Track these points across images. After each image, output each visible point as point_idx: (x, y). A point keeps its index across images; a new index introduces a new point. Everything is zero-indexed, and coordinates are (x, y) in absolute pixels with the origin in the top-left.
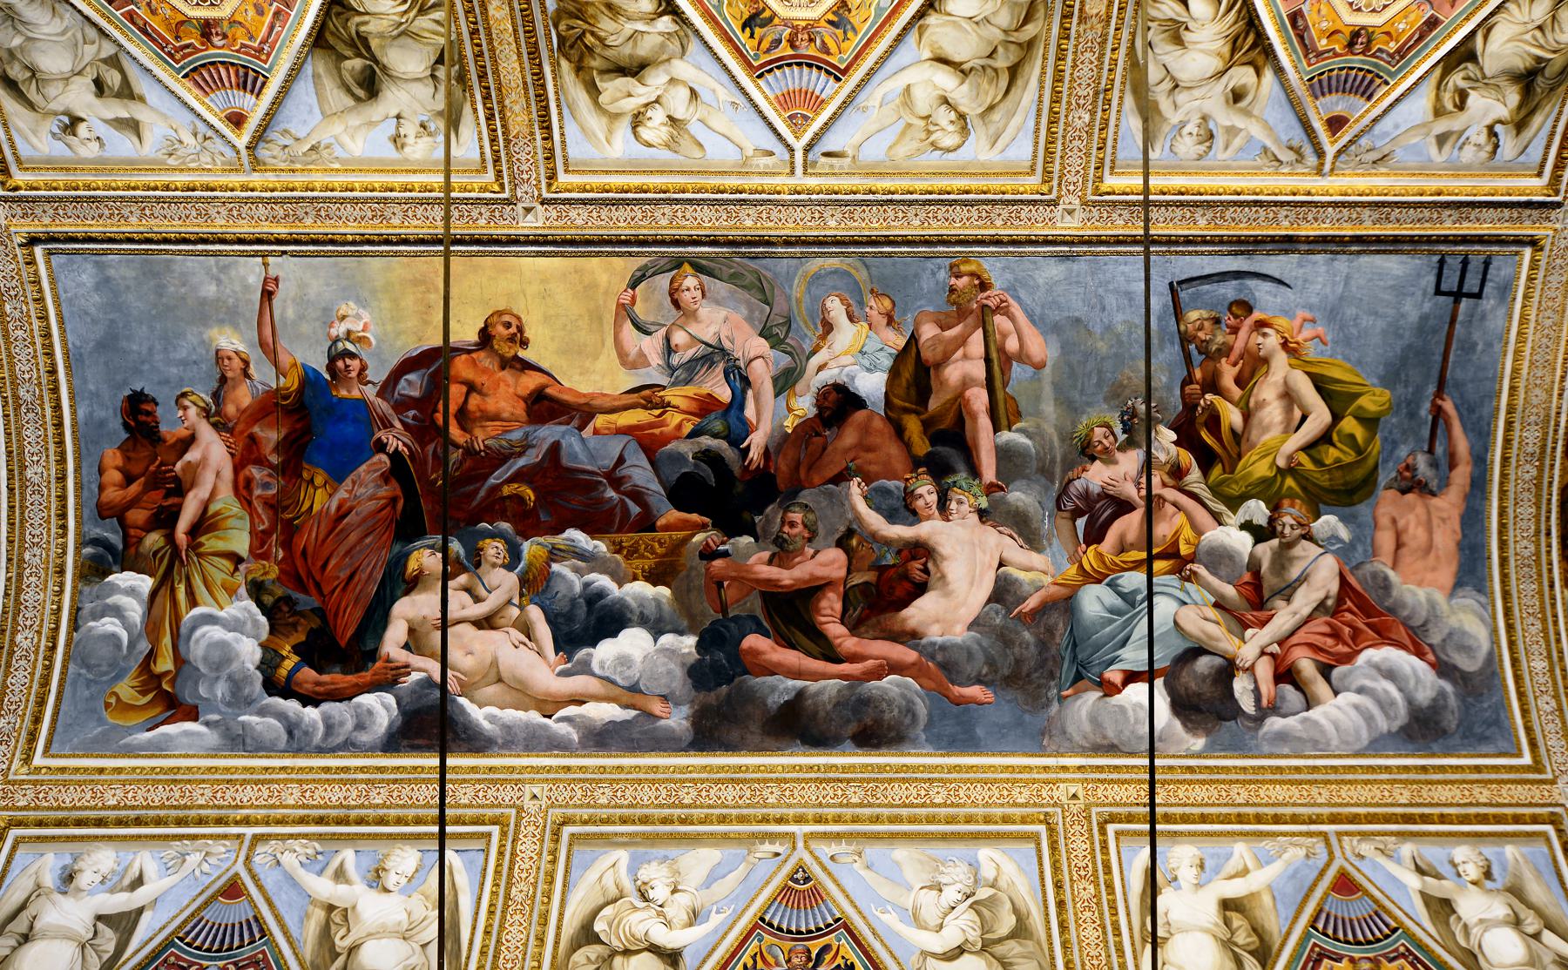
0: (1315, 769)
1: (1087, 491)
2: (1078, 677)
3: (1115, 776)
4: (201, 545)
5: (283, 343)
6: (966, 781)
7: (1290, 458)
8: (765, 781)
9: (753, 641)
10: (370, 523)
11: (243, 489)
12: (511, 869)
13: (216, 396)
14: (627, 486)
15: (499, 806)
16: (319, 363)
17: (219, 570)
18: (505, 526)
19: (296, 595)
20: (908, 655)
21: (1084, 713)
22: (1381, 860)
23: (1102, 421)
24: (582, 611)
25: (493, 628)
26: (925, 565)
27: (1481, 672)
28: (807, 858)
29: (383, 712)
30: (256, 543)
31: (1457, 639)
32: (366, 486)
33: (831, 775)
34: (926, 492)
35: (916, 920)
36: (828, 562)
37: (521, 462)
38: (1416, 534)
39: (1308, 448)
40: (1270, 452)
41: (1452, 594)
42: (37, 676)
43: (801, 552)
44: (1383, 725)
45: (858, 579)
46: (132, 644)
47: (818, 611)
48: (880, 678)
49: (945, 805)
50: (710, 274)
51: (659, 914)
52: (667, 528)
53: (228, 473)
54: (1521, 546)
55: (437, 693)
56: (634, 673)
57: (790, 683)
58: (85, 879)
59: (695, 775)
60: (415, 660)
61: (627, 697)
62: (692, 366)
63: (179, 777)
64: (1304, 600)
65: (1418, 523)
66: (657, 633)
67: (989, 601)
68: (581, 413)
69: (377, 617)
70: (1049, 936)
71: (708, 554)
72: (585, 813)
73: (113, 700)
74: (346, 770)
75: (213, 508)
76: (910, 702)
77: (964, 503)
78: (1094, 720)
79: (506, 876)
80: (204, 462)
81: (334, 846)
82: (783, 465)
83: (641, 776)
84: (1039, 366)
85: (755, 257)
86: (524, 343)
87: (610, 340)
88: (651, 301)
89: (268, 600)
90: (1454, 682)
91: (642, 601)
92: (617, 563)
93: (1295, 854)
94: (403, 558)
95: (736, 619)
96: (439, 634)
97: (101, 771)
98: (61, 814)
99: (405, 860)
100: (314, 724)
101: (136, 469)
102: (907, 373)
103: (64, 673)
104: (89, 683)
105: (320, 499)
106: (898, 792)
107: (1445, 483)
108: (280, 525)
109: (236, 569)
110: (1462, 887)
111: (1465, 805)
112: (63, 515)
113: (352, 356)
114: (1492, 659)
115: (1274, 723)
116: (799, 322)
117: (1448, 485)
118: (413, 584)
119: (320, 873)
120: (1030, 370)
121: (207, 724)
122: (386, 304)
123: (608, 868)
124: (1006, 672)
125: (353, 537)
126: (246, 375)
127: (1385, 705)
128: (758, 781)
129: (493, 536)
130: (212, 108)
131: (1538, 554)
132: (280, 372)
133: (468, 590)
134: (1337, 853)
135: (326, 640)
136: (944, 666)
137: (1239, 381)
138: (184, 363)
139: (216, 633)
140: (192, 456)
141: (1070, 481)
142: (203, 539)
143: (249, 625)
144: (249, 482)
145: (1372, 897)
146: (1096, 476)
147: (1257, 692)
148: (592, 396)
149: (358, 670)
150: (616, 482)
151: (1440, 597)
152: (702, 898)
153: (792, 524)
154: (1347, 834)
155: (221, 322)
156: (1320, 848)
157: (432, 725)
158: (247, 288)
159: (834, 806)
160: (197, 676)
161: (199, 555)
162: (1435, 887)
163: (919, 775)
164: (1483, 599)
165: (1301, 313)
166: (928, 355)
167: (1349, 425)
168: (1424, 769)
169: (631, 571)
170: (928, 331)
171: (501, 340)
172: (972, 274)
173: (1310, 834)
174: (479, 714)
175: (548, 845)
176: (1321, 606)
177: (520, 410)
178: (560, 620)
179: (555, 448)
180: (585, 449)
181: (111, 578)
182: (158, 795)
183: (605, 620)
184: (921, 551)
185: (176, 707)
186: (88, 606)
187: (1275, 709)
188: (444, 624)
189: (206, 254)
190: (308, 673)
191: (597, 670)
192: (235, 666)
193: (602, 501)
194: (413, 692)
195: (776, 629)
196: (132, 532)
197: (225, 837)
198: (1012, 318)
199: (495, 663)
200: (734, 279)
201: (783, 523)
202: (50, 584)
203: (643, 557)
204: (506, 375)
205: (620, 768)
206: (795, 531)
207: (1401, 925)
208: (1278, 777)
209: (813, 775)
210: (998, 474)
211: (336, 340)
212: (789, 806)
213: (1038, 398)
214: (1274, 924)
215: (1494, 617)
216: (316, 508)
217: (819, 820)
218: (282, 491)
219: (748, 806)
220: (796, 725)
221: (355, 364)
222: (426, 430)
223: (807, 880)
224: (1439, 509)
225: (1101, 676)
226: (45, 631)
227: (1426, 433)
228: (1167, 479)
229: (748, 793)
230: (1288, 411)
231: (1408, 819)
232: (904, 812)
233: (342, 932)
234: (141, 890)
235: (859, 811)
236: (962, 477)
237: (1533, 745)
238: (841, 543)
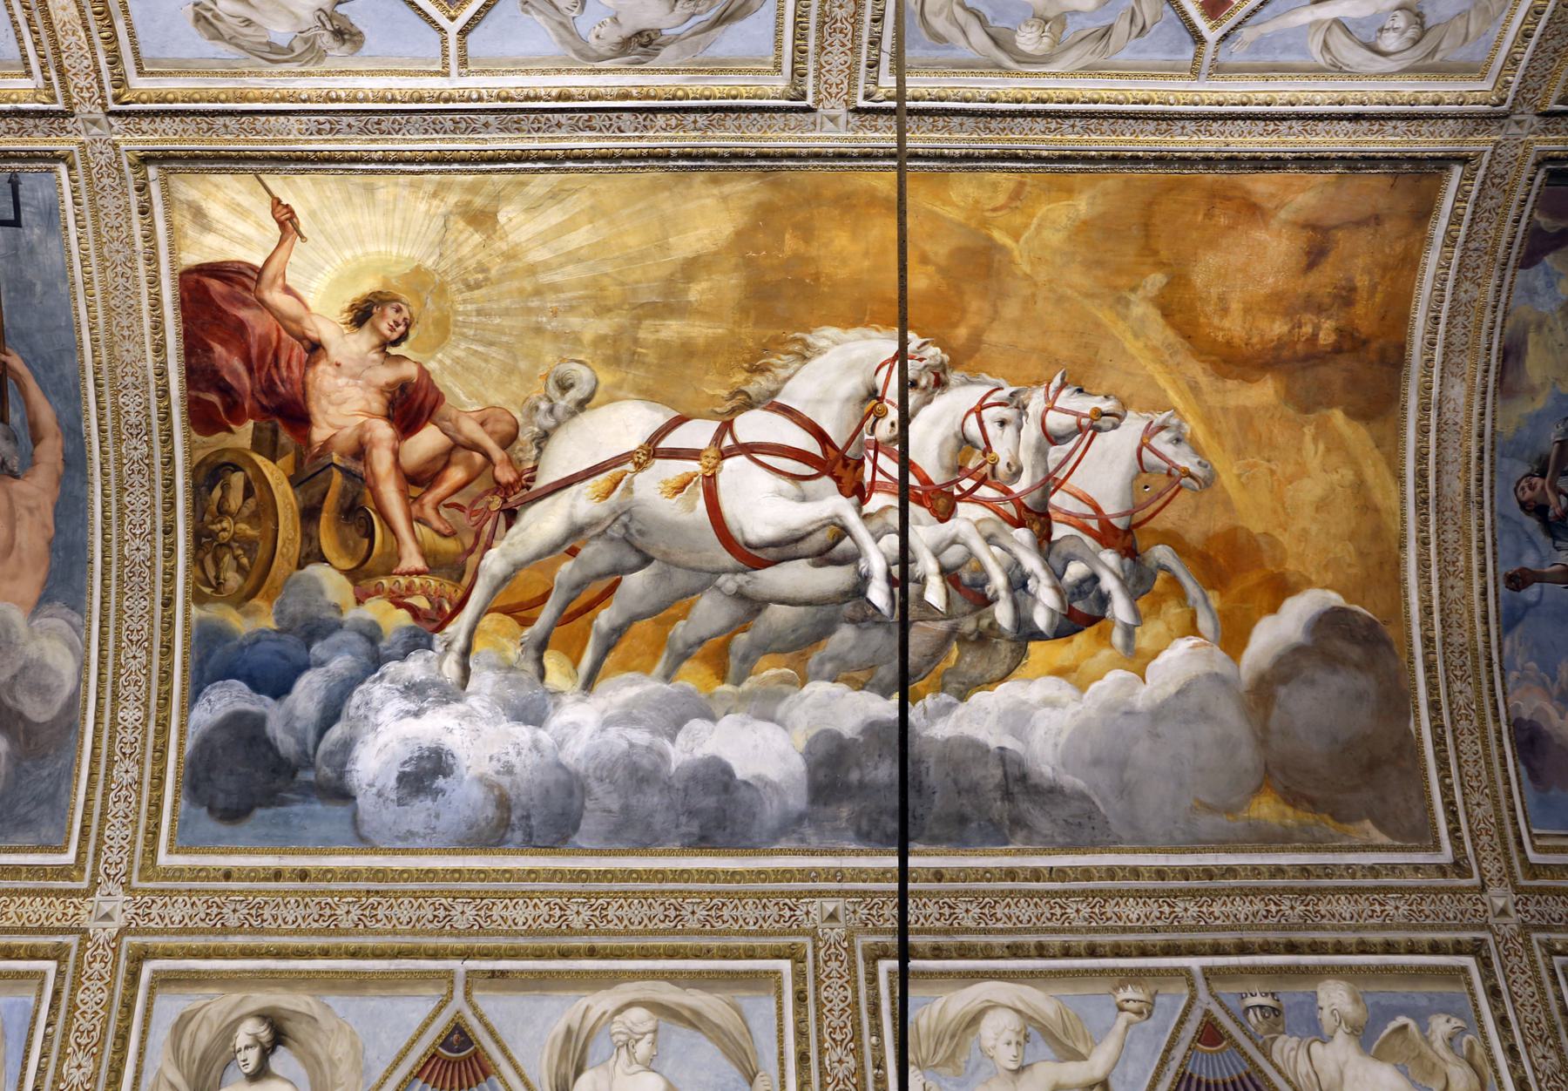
27: (54, 723)
41: (34, 613)
107: (31, 462)
114: (74, 705)
117: (33, 464)
164: (76, 619)
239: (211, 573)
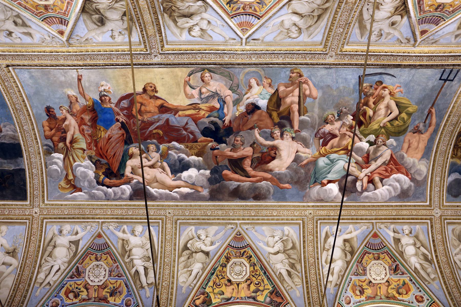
0: (374, 206)
1: (324, 132)
2: (315, 182)
3: (322, 208)
4: (73, 146)
5: (86, 93)
6: (282, 210)
7: (385, 124)
8: (229, 209)
9: (226, 172)
10: (118, 140)
11: (82, 132)
12: (165, 232)
13: (70, 107)
14: (189, 130)
15: (161, 215)
16: (97, 98)
17: (80, 153)
18: (155, 141)
19: (101, 159)
20: (268, 176)
21: (315, 191)
22: (385, 229)
23: (331, 112)
24: (178, 164)
25: (154, 168)
26: (275, 152)
27: (422, 180)
28: (240, 230)
29: (128, 190)
30: (88, 146)
31: (418, 172)
32: (115, 131)
33: (247, 208)
34: (277, 132)
35: (268, 245)
36: (247, 151)
37: (158, 124)
38: (415, 144)
39: (390, 121)
40: (379, 122)
41: (420, 160)
42: (40, 181)
43: (240, 148)
44: (393, 194)
45: (256, 156)
46: (62, 172)
47: (244, 164)
48: (261, 182)
49: (276, 216)
50: (214, 72)
51: (203, 243)
52: (201, 142)
53: (77, 127)
54: (442, 147)
55: (142, 185)
56: (193, 180)
57: (236, 183)
58: (64, 232)
59: (211, 208)
60: (135, 176)
61: (192, 186)
62: (208, 99)
63: (81, 207)
64: (380, 162)
65: (416, 141)
66: (199, 169)
67: (293, 162)
68: (175, 111)
69: (123, 165)
70: (300, 249)
71: (213, 149)
72: (183, 217)
73: (60, 186)
74: (121, 205)
75: (75, 137)
76: (269, 188)
77: (288, 135)
78: (318, 193)
79: (164, 233)
80: (70, 124)
81: (121, 225)
82: (234, 125)
83: (197, 208)
84: (315, 98)
85: (229, 68)
86: (156, 92)
87: (182, 91)
88: (195, 79)
89: (94, 161)
90: (414, 183)
91: (194, 161)
92: (187, 151)
93: (364, 227)
94: (127, 150)
95: (221, 166)
96: (141, 170)
97: (62, 205)
98: (55, 216)
99: (139, 228)
100: (111, 193)
101: (52, 126)
102: (274, 100)
103: (47, 179)
104: (53, 182)
105: (104, 134)
106: (264, 213)
108: (94, 141)
109: (84, 152)
110: (403, 236)
111: (409, 215)
112: (36, 139)
113: (106, 96)
115: (366, 194)
116: (241, 86)
118: (131, 156)
119: (119, 231)
120: (312, 100)
121: (85, 193)
122: (114, 82)
123: (190, 231)
124: (296, 180)
125: (113, 144)
126: (77, 101)
127: (395, 189)
128: (227, 209)
129: (152, 144)
130: (53, 30)
131: (446, 150)
132: (87, 100)
133: (146, 158)
134: (375, 228)
135: (111, 172)
136: (278, 179)
137: (374, 103)
138: (59, 98)
139: (82, 169)
140: (67, 123)
141: (320, 129)
142: (74, 145)
143: (90, 167)
144: (83, 130)
145: (381, 238)
146: (328, 128)
147: (362, 186)
148: (178, 106)
149: (120, 179)
150: (186, 129)
151: (416, 161)
152: (214, 239)
153: (237, 141)
154: (378, 222)
155: (67, 87)
156: (371, 226)
157: (141, 193)
158: (73, 78)
159: (247, 216)
160: (80, 181)
161: (74, 149)
162: (397, 236)
163: (270, 208)
164: (428, 161)
165: (397, 85)
166: (281, 95)
167: (404, 115)
168: (401, 206)
169: (191, 153)
170: (282, 89)
171: (149, 91)
172: (297, 73)
173: (369, 223)
174: (153, 190)
175: (174, 226)
176: (384, 163)
177: (157, 110)
178: (172, 166)
179: (167, 120)
180: (176, 120)
181: (52, 155)
182: (77, 212)
183: (185, 166)
184: (275, 148)
185: (76, 188)
186: (48, 162)
187: (366, 190)
188: (142, 167)
189: (60, 69)
190: (107, 180)
191: (183, 179)
192: (88, 178)
193: (181, 134)
194: (135, 185)
195: (232, 169)
196: (55, 143)
197: (95, 222)
198: (308, 85)
199: (155, 177)
200: (221, 74)
201: (235, 140)
202: (38, 157)
203: (194, 149)
204: (152, 100)
205: (191, 206)
206: (238, 142)
207: (387, 245)
208: (364, 208)
209: (242, 208)
210: (299, 127)
211: (101, 92)
212: (236, 216)
213: (313, 107)
214: (356, 245)
215: (430, 166)
216: (102, 136)
217: (243, 219)
218: (92, 132)
219: (225, 216)
220: (237, 194)
221: (107, 98)
222: (130, 116)
223: (240, 235)
224: (423, 137)
225: (321, 181)
226: (39, 169)
227: (425, 117)
228: (348, 129)
229: (225, 213)
230: (387, 111)
231: (394, 219)
232: (266, 218)
233: (127, 246)
235: (254, 217)
236: (288, 128)
237: (430, 200)
238: (251, 146)
239: (455, 153)
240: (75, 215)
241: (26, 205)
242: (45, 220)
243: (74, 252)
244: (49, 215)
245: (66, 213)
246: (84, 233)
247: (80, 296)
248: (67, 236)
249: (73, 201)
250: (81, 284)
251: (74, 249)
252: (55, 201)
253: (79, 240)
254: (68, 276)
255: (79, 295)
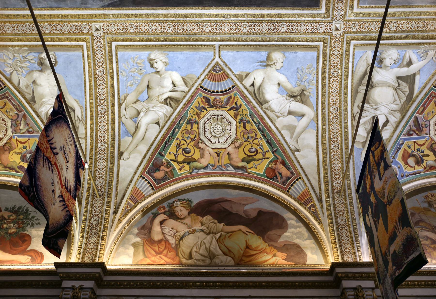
63: (422, 17)
182: (413, 26)
234: (412, 67)
240: (409, 31)
241: (320, 16)
242: (353, 43)
243: (407, 94)
244: (361, 32)
245: (393, 29)
246: (422, 63)
247: (425, 162)
248: (392, 68)
249: (406, 7)
250: (424, 144)
251: (407, 89)
252: (372, 7)
253: (414, 75)
254: (405, 132)
255: (422, 161)
